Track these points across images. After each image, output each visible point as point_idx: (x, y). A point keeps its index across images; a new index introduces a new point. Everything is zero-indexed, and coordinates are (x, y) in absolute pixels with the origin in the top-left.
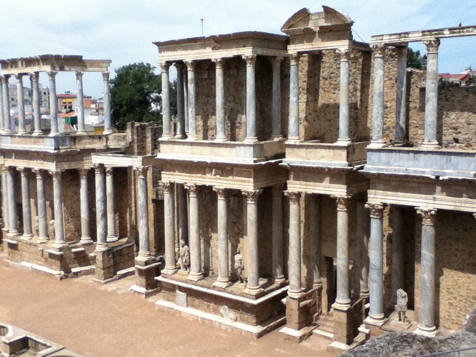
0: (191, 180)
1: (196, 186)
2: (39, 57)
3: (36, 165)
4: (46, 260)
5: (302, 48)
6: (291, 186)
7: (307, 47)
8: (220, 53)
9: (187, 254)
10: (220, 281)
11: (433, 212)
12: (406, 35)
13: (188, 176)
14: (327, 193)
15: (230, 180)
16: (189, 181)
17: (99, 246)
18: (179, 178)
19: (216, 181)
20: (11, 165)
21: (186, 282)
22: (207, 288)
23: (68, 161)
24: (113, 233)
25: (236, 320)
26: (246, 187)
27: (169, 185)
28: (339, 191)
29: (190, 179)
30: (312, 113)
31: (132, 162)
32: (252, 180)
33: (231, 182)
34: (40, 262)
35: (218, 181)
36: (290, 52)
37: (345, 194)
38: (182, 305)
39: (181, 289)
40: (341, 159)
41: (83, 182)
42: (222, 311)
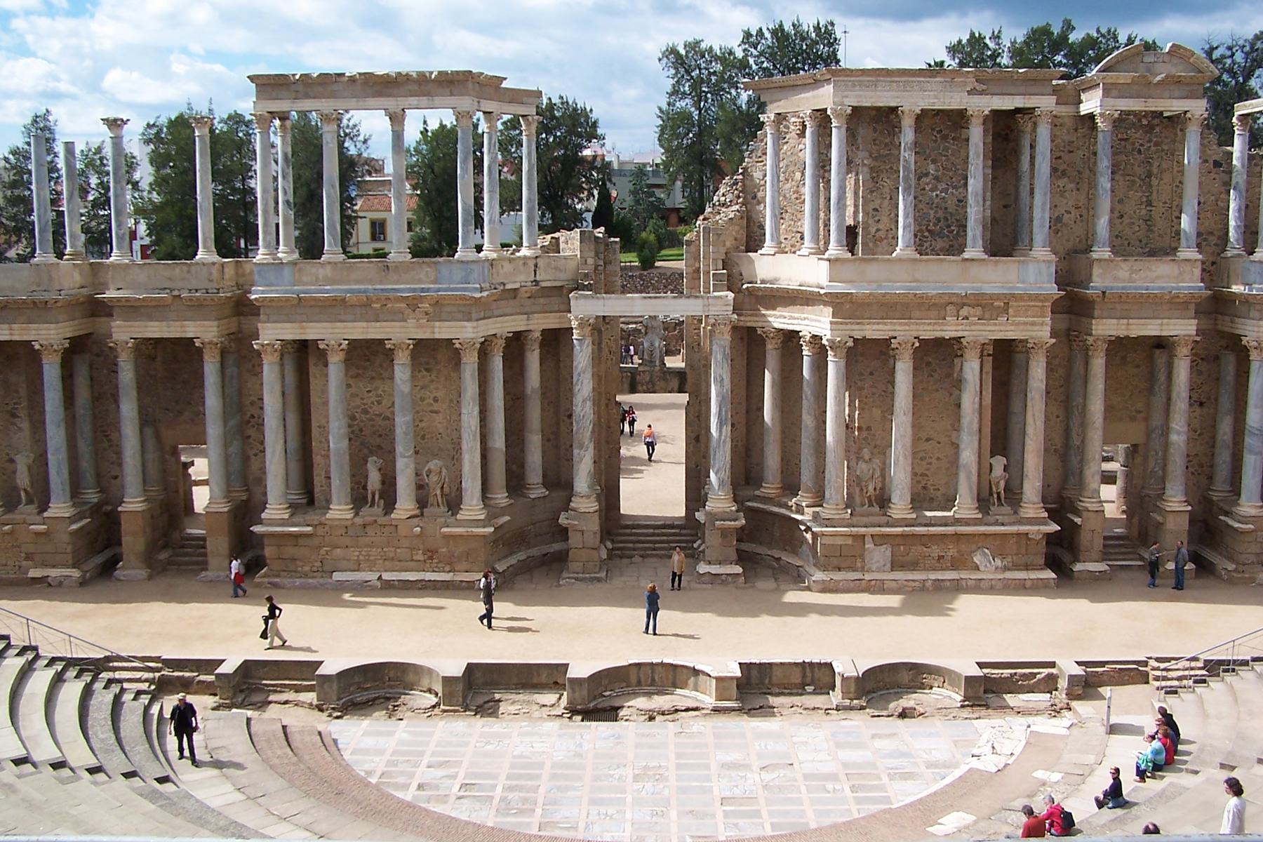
0: (904, 332)
2: (414, 75)
3: (399, 332)
4: (431, 554)
9: (878, 474)
10: (964, 506)
13: (900, 324)
17: (584, 499)
20: (289, 337)
21: (888, 525)
23: (484, 318)
24: (541, 480)
25: (1006, 569)
27: (850, 344)
28: (1183, 328)
30: (1073, 210)
33: (1003, 328)
34: (402, 564)
35: (973, 328)
38: (879, 570)
39: (880, 540)
40: (1191, 281)
41: (497, 364)
42: (977, 559)
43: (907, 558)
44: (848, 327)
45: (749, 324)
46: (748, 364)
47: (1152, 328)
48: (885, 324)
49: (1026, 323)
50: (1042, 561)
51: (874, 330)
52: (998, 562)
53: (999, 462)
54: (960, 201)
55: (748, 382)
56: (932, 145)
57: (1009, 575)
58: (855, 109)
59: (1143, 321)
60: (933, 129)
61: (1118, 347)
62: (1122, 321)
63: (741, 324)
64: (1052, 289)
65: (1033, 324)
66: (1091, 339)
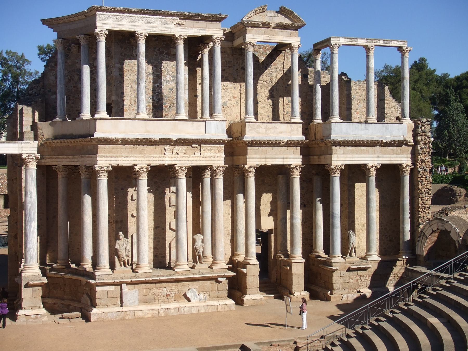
0: (142, 160)
1: (152, 167)
5: (260, 38)
6: (251, 160)
7: (265, 38)
8: (185, 30)
11: (379, 167)
12: (356, 40)
13: (139, 157)
14: (285, 163)
15: (197, 157)
16: (140, 162)
18: (124, 158)
19: (178, 159)
22: (167, 276)
26: (216, 162)
27: (110, 169)
29: (143, 159)
31: (20, 150)
32: (223, 155)
35: (181, 159)
36: (247, 41)
37: (301, 163)
43: (147, 297)
44: (109, 159)
45: (47, 164)
46: (48, 190)
47: (279, 161)
48: (130, 157)
49: (210, 157)
50: (226, 295)
51: (124, 161)
52: (202, 296)
53: (199, 237)
54: (170, 89)
55: (48, 201)
56: (154, 57)
57: (208, 303)
58: (110, 31)
59: (273, 156)
60: (155, 48)
61: (261, 171)
62: (262, 156)
63: (43, 164)
64: (225, 137)
65: (214, 157)
66: (246, 167)
